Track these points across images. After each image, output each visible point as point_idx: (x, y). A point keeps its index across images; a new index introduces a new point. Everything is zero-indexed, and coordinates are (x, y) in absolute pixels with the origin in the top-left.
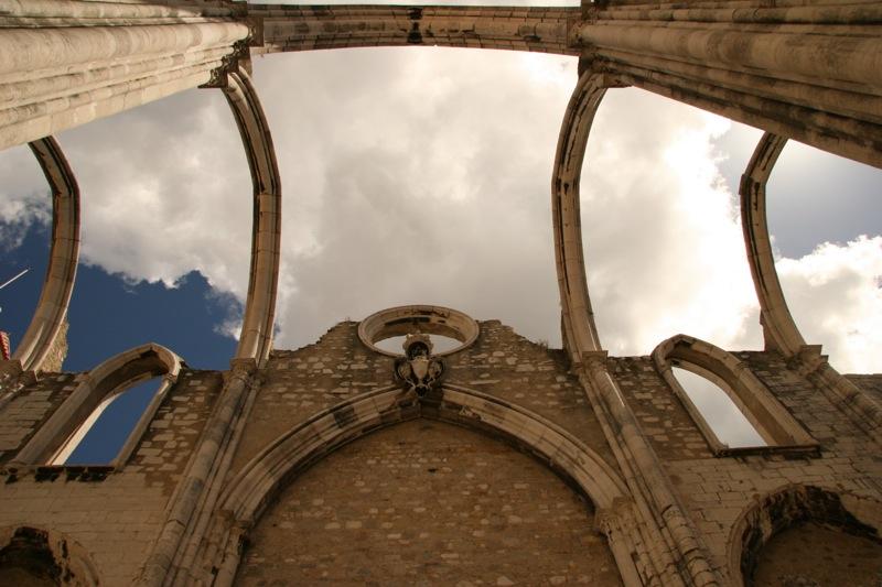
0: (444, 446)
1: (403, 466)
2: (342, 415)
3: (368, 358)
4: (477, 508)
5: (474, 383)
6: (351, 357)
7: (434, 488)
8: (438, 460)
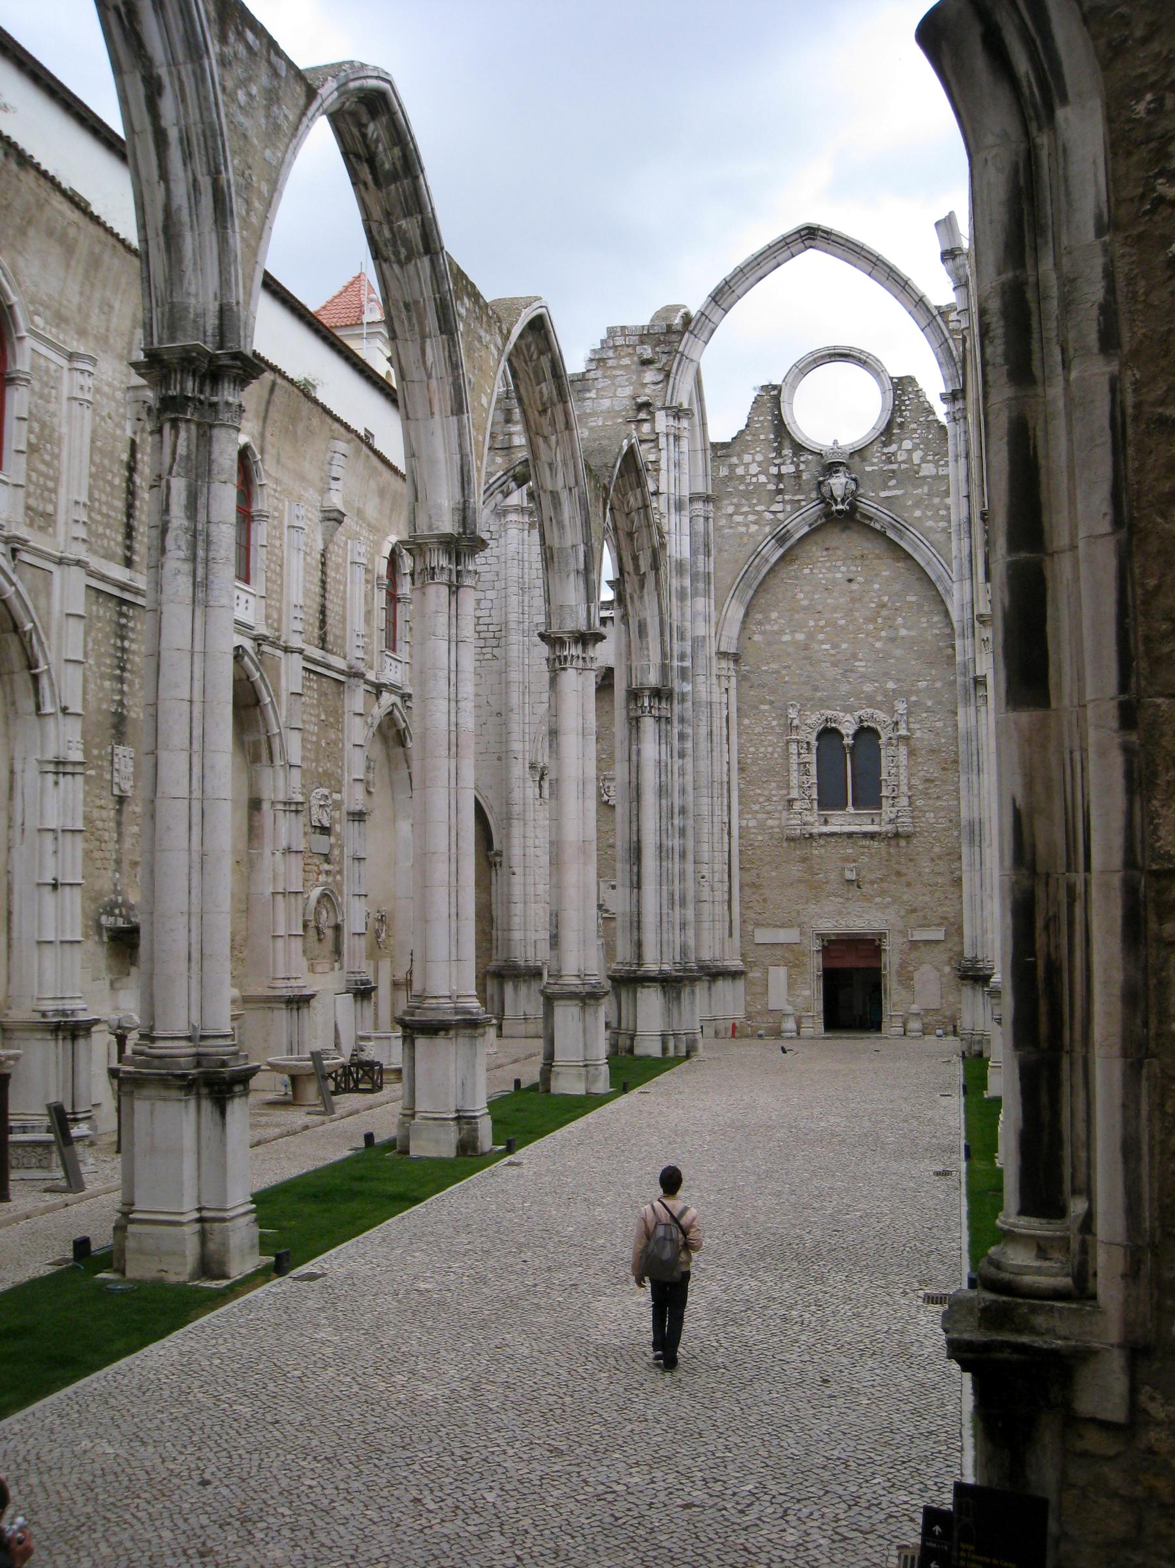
0: (857, 553)
1: (829, 575)
3: (795, 454)
4: (880, 620)
5: (883, 494)
7: (853, 600)
8: (854, 568)
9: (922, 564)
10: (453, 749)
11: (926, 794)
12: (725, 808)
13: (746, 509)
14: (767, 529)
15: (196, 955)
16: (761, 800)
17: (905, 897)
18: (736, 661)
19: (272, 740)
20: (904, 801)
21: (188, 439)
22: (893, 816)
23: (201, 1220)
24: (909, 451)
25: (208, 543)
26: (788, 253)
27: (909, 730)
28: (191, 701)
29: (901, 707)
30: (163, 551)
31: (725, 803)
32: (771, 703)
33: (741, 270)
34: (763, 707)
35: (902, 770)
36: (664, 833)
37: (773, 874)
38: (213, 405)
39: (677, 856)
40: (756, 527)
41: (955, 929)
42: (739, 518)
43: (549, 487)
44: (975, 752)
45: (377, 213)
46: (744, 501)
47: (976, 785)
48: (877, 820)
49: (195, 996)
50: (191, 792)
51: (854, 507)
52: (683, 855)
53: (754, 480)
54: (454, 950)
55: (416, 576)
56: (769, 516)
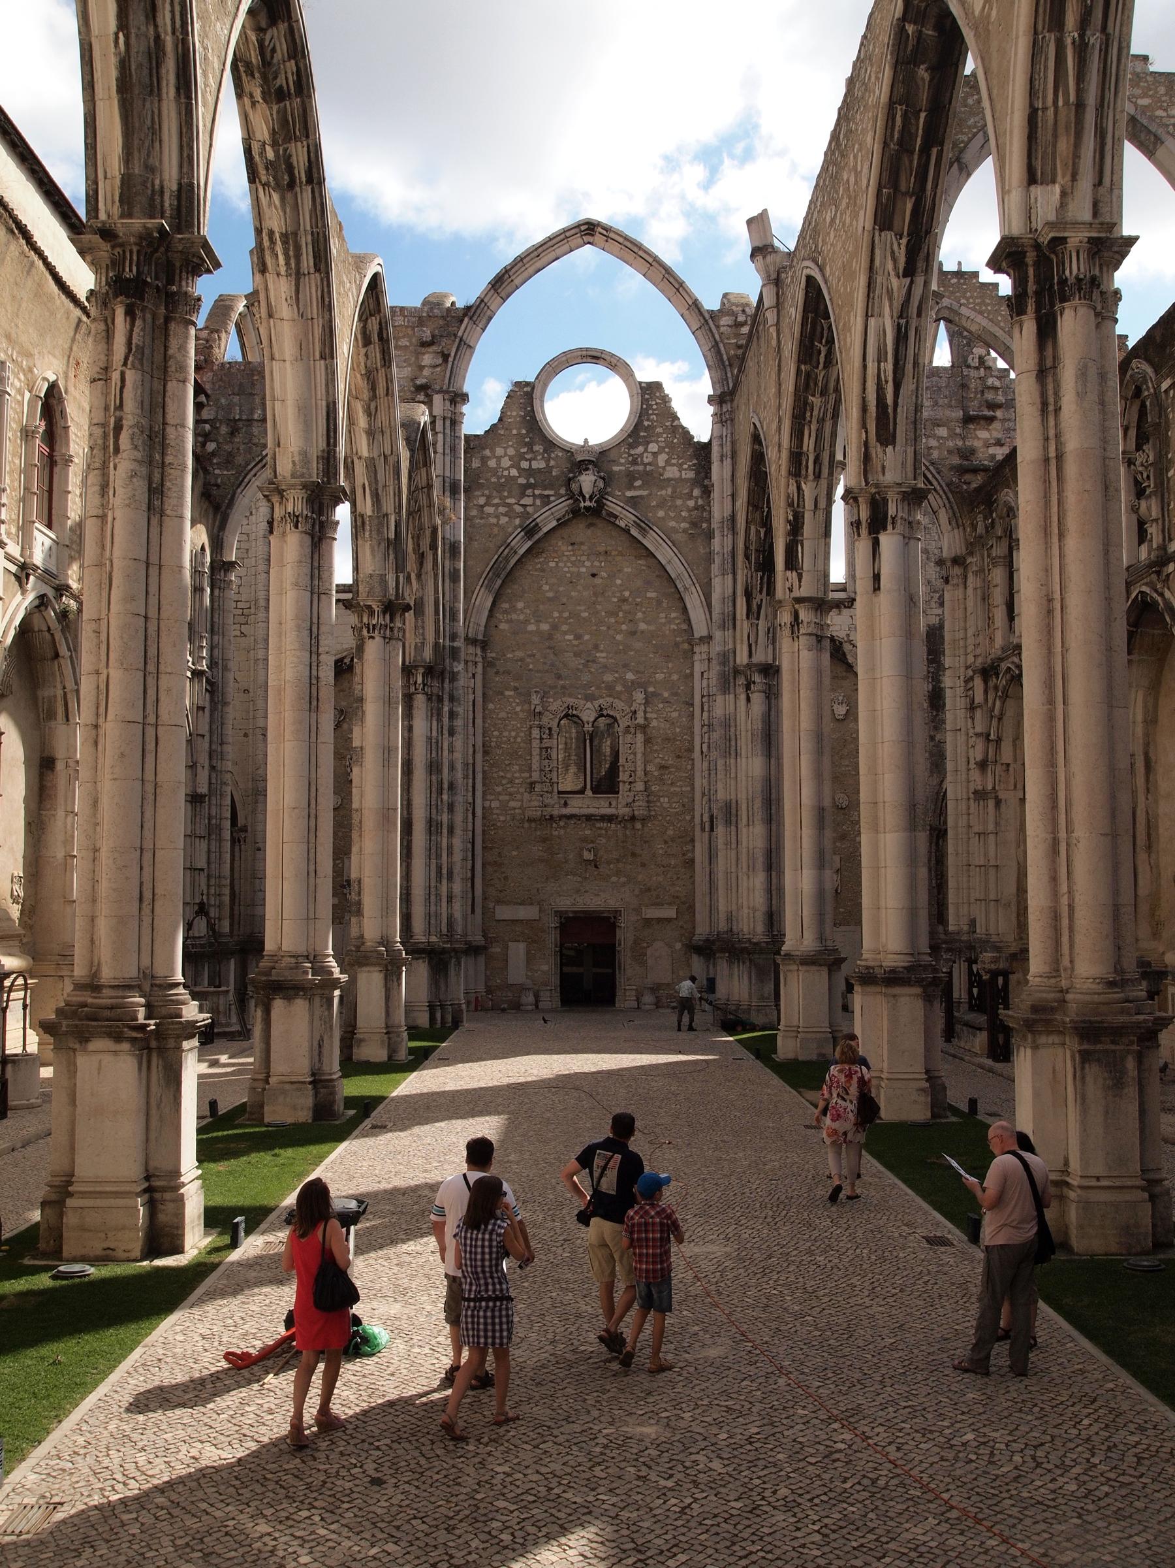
0: (602, 549)
2: (530, 531)
3: (545, 451)
4: (621, 614)
5: (629, 494)
6: (530, 446)
8: (596, 563)
9: (663, 562)
10: (314, 703)
11: (661, 780)
12: (470, 789)
13: (496, 501)
14: (517, 521)
15: (148, 895)
16: (504, 782)
17: (640, 877)
18: (483, 649)
19: (69, 696)
20: (640, 786)
21: (143, 330)
22: (630, 800)
23: (149, 1190)
24: (655, 454)
25: (164, 447)
26: (566, 247)
27: (646, 719)
28: (146, 617)
29: (639, 696)
30: (117, 450)
31: (470, 784)
32: (516, 689)
33: (522, 260)
34: (507, 693)
35: (639, 756)
36: (434, 807)
37: (515, 853)
38: (170, 296)
39: (445, 831)
40: (507, 519)
41: (687, 908)
42: (489, 510)
43: (365, 452)
44: (733, 737)
45: (263, 132)
46: (495, 493)
47: (733, 770)
48: (614, 803)
49: (146, 940)
50: (145, 717)
51: (600, 505)
52: (451, 831)
53: (506, 473)
54: (311, 906)
55: (275, 524)
56: (518, 509)
